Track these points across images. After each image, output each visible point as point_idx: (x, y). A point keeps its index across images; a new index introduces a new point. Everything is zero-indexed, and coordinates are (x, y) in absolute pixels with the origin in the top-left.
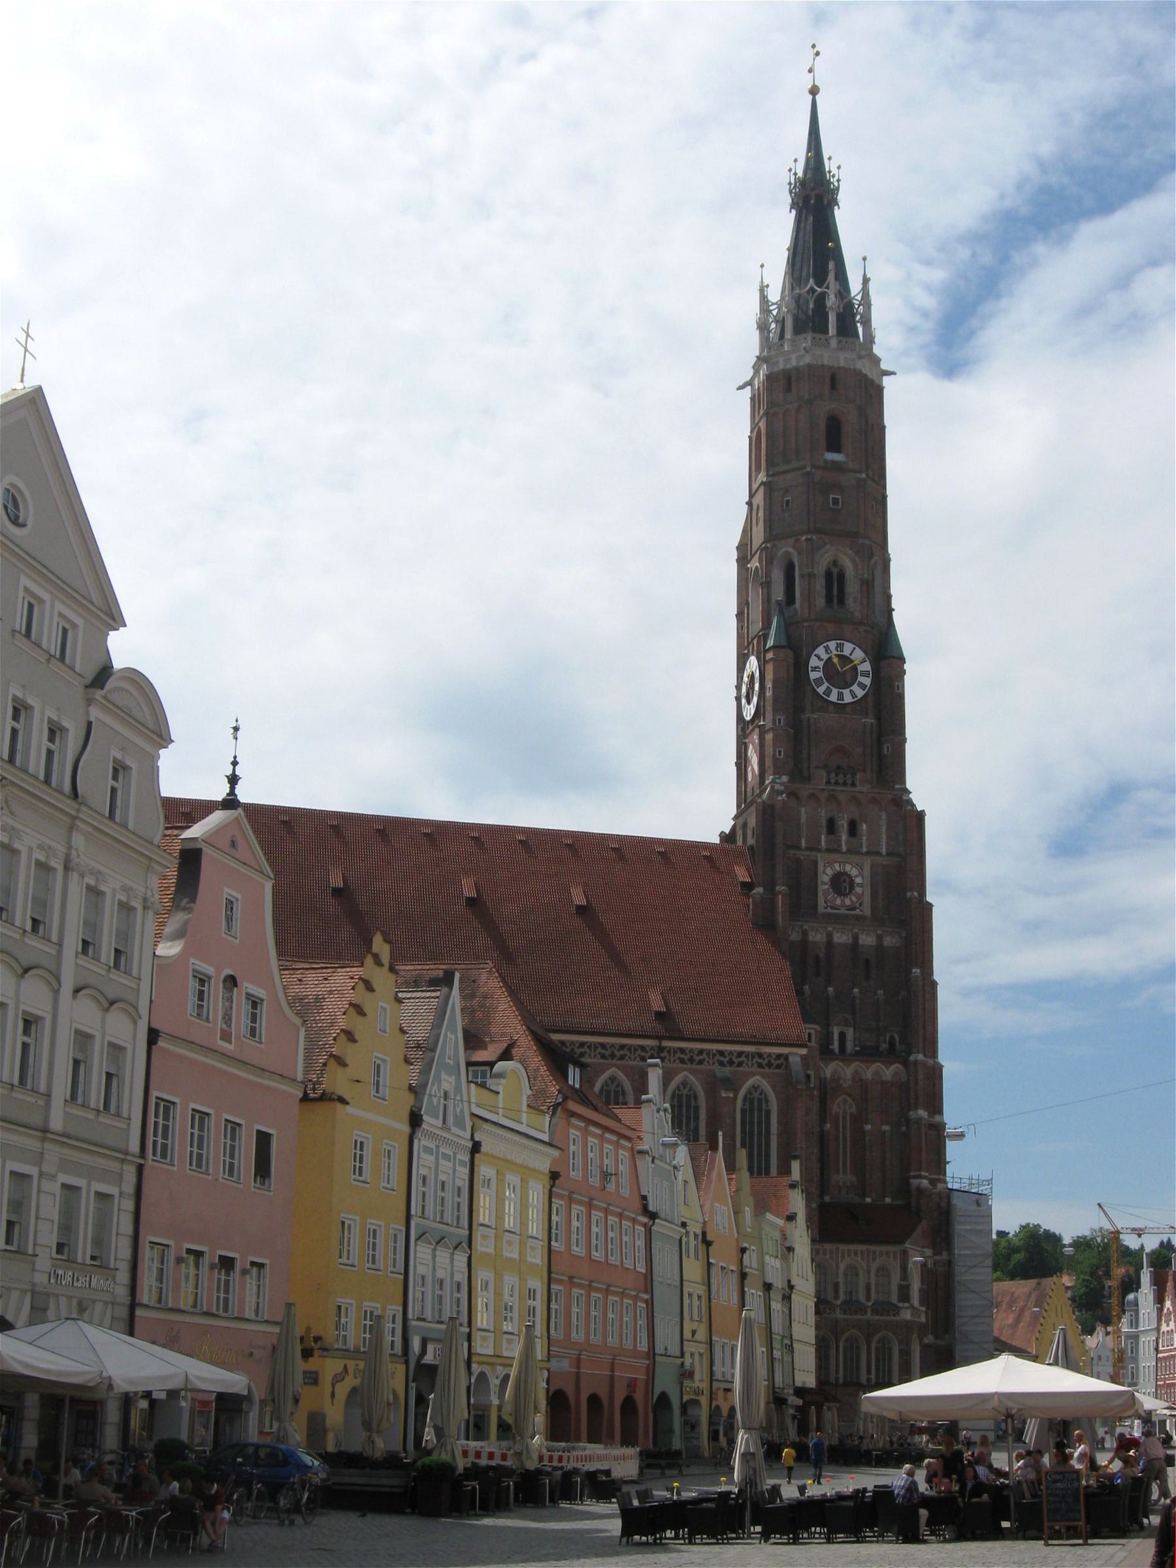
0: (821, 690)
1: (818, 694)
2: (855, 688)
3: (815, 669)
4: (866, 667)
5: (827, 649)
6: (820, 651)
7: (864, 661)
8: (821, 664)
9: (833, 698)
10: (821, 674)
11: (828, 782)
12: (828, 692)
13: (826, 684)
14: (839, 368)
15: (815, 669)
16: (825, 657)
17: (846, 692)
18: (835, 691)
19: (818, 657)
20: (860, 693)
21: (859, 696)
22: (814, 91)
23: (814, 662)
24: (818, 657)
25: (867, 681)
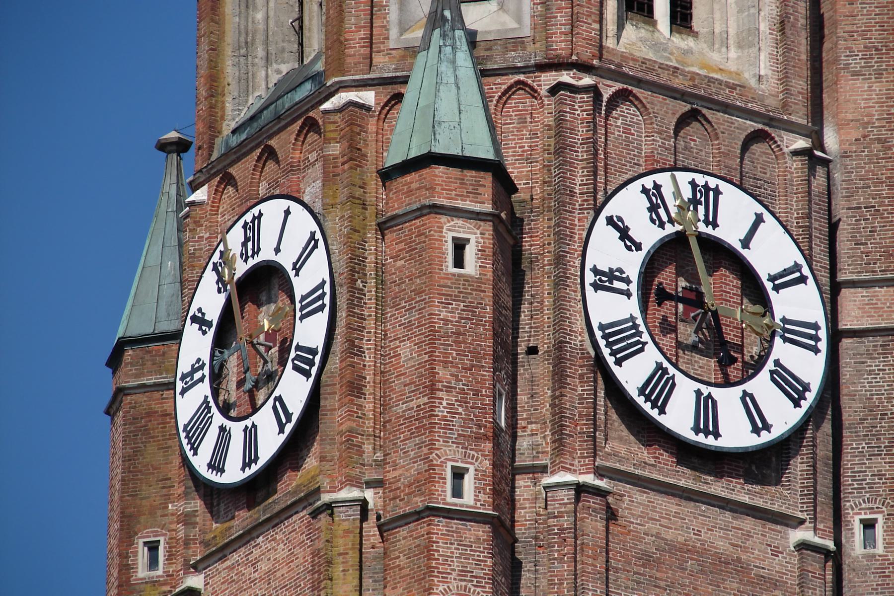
0: (632, 375)
1: (615, 391)
2: (761, 385)
3: (608, 280)
5: (655, 200)
6: (629, 204)
7: (789, 278)
12: (659, 388)
15: (608, 280)
16: (649, 235)
17: (728, 399)
18: (685, 392)
19: (624, 234)
20: (783, 416)
24: (624, 234)
25: (810, 367)
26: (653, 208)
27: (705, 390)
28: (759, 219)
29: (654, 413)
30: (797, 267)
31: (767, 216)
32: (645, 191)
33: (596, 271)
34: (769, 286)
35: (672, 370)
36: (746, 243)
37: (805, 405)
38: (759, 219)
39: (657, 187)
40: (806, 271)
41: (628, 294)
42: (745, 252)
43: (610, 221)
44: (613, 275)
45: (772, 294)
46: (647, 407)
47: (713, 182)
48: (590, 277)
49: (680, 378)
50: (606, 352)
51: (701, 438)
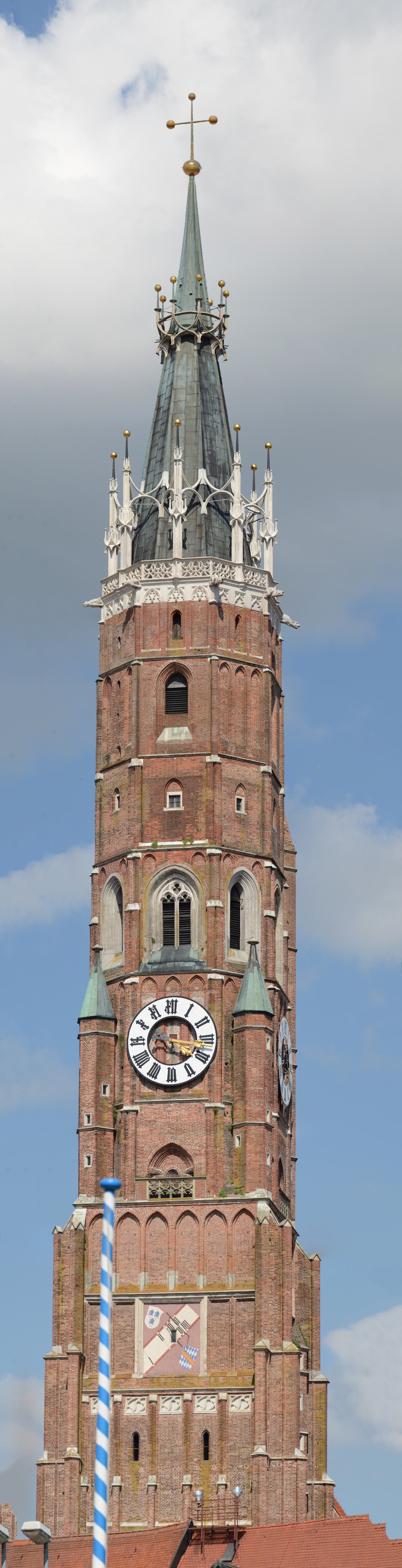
0: (144, 1070)
3: (137, 1041)
4: (208, 1029)
5: (154, 1012)
7: (205, 1021)
8: (145, 1034)
9: (162, 1078)
10: (145, 1048)
11: (154, 1195)
13: (152, 1061)
14: (184, 604)
15: (137, 1041)
16: (151, 1023)
18: (164, 1069)
19: (143, 1025)
21: (197, 1074)
22: (192, 171)
23: (136, 1031)
24: (143, 1025)
26: (153, 1014)
27: (171, 1067)
28: (192, 1006)
29: (153, 1080)
30: (206, 1018)
31: (195, 1004)
32: (150, 1009)
33: (132, 1040)
34: (195, 1027)
35: (159, 1064)
36: (186, 1016)
37: (208, 1062)
38: (192, 1006)
39: (154, 1006)
40: (209, 1018)
41: (144, 1044)
42: (187, 1019)
43: (138, 1022)
44: (138, 1039)
45: (196, 1029)
46: (150, 1078)
47: (174, 999)
48: (130, 1042)
49: (162, 1066)
50: (136, 1065)
51: (170, 1083)
